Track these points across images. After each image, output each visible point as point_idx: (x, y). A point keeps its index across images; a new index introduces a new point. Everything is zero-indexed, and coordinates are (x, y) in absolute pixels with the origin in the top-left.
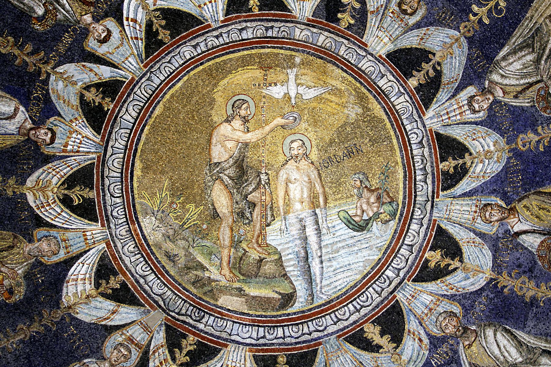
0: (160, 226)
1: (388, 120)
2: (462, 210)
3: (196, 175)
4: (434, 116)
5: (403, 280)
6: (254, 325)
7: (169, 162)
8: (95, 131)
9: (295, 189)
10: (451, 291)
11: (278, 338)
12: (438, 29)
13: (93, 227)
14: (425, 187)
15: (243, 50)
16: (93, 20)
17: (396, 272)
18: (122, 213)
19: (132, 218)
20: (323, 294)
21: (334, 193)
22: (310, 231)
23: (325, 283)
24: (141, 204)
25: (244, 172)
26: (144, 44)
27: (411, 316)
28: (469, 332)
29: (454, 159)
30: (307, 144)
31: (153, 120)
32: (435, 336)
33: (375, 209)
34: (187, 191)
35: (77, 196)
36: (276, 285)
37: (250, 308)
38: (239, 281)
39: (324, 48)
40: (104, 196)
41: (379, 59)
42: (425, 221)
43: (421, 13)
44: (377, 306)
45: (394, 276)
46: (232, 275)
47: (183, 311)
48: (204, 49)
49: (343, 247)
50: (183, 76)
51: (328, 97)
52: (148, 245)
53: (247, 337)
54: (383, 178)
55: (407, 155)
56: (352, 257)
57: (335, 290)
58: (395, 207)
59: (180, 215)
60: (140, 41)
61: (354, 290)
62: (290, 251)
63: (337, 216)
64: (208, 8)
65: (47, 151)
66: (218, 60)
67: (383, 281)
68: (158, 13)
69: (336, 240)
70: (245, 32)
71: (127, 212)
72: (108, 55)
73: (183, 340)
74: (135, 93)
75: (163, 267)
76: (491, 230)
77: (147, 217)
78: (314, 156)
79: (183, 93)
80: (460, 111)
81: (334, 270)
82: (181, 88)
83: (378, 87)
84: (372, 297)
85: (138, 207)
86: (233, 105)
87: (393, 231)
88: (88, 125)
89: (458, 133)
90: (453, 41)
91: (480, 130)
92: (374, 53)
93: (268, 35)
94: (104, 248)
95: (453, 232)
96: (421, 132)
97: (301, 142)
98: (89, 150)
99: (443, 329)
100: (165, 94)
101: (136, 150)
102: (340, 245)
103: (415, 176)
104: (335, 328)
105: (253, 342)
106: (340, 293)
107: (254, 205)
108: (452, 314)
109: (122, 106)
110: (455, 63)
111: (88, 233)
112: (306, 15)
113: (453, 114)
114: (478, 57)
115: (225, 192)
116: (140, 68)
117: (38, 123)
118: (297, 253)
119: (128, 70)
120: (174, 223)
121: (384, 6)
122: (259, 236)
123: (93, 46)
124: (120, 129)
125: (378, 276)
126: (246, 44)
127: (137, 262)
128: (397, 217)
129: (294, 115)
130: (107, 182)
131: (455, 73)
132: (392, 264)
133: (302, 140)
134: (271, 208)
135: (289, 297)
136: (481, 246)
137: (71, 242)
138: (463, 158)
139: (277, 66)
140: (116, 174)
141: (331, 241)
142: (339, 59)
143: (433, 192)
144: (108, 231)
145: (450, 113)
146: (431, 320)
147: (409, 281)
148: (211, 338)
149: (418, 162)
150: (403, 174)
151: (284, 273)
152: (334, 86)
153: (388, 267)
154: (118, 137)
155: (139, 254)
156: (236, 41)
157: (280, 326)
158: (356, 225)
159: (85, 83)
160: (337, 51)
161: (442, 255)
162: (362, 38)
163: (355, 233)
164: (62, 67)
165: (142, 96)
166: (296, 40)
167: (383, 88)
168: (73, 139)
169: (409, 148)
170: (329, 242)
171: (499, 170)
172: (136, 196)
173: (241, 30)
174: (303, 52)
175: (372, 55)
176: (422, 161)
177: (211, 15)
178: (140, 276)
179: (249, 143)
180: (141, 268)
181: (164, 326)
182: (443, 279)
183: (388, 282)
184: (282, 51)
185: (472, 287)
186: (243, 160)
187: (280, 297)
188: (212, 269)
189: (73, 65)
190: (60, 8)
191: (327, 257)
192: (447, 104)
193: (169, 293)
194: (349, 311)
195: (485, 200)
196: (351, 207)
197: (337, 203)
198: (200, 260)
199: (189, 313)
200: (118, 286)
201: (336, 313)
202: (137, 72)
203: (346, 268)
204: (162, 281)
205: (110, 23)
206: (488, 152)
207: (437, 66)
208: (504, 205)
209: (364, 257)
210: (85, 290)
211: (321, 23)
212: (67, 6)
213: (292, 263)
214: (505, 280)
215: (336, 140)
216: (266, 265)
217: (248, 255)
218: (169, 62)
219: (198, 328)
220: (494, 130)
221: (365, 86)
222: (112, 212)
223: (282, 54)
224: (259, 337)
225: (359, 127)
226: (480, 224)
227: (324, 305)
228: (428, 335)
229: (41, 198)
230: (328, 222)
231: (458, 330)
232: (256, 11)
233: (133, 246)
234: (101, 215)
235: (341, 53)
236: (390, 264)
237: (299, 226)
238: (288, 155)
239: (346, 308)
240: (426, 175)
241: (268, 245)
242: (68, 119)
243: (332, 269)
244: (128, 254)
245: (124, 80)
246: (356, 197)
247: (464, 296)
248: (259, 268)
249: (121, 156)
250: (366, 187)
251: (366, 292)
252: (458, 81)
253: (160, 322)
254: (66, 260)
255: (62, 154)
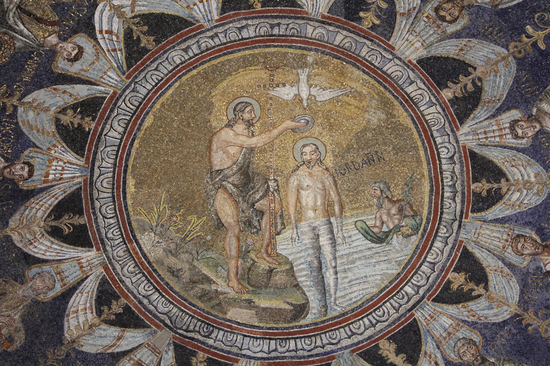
0: (160, 241)
1: (415, 130)
2: (492, 235)
3: (196, 184)
4: (469, 132)
5: (423, 297)
6: (266, 338)
7: (166, 173)
8: (78, 154)
9: (308, 197)
10: (472, 318)
11: (290, 351)
12: (481, 43)
13: (89, 253)
14: (453, 205)
15: (244, 50)
16: (60, 39)
17: (416, 289)
18: (118, 234)
19: (129, 236)
20: (337, 305)
21: (350, 201)
22: (324, 241)
23: (339, 294)
24: (137, 220)
25: (250, 179)
26: (124, 54)
27: (429, 338)
28: (487, 363)
29: (488, 182)
30: (322, 149)
31: (143, 132)
32: (452, 362)
33: (396, 222)
34: (186, 202)
35: (67, 226)
36: (288, 296)
37: (261, 320)
38: (248, 292)
39: (342, 48)
40: (96, 219)
41: (408, 64)
42: (451, 241)
43: (462, 23)
44: (394, 323)
45: (413, 292)
46: (240, 287)
47: (191, 328)
48: (197, 51)
49: (360, 258)
50: (173, 83)
51: (346, 99)
52: (149, 262)
53: (259, 350)
54: (407, 189)
55: (435, 169)
56: (369, 269)
57: (349, 302)
58: (418, 221)
59: (181, 228)
60: (119, 52)
61: (370, 303)
62: (303, 261)
63: (354, 226)
64: (199, 8)
65: (24, 186)
66: (214, 62)
67: (401, 297)
68: (137, 20)
69: (352, 250)
70: (245, 30)
71: (123, 231)
72: (83, 73)
73: (193, 358)
74: (119, 107)
75: (167, 284)
76: (523, 263)
77: (146, 234)
78: (329, 161)
79: (176, 101)
80: (500, 134)
81: (350, 282)
82: (172, 96)
83: (406, 93)
84: (389, 312)
85: (134, 224)
86: (235, 110)
87: (414, 246)
88: (68, 150)
89: (496, 156)
90: (499, 58)
91: (522, 158)
92: (402, 57)
93: (274, 33)
94: (102, 272)
95: (480, 256)
96: (452, 147)
97: (314, 147)
98: (73, 175)
99: (461, 355)
100: (154, 103)
101: (126, 166)
102: (356, 256)
103: (443, 193)
104: (349, 342)
105: (265, 355)
106: (355, 306)
107: (261, 213)
108: (471, 342)
109: (105, 124)
110: (500, 82)
111: (83, 261)
112: (320, 11)
113: (492, 134)
114: (527, 81)
115: (229, 201)
116: (122, 81)
117: (11, 161)
118: (310, 264)
119: (108, 85)
120: (176, 237)
121: (417, 10)
122: (268, 246)
123: (64, 67)
124: (106, 147)
125: (396, 291)
126: (246, 44)
127: (139, 282)
128: (420, 232)
129: (306, 118)
130: (97, 204)
131: (498, 93)
132: (412, 280)
133: (315, 145)
134: (281, 216)
135: (301, 308)
136: (509, 277)
137: (66, 274)
138: (498, 183)
139: (285, 65)
140: (106, 195)
141: (347, 252)
142: (360, 60)
143: (462, 212)
144: (104, 255)
145: (489, 132)
146: (449, 344)
147: (428, 300)
148: (221, 353)
149: (447, 178)
150: (429, 188)
151: (295, 283)
152: (353, 88)
153: (407, 283)
154: (104, 156)
155: (140, 273)
156: (235, 41)
157: (292, 338)
158: (375, 236)
159: (60, 107)
160: (357, 52)
161: (466, 279)
162: (389, 40)
163: (373, 245)
164: (29, 96)
165: (128, 109)
166: (309, 38)
167: (412, 95)
168: (54, 168)
169: (438, 162)
170: (344, 253)
171: (538, 203)
172: (131, 214)
173: (240, 29)
174: (316, 51)
175: (400, 59)
176: (452, 178)
177: (203, 16)
178: (144, 296)
179: (255, 147)
180: (144, 288)
181: (172, 345)
182: (466, 304)
183: (406, 298)
184: (292, 50)
185: (495, 318)
186: (248, 167)
187: (292, 308)
188: (220, 281)
189: (42, 91)
190: (17, 35)
191: (342, 268)
192: (486, 123)
193: (175, 310)
194: (365, 325)
195: (518, 231)
196: (369, 217)
197: (355, 212)
198: (205, 273)
199: (197, 329)
200: (121, 310)
201: (351, 326)
202: (119, 85)
203: (362, 281)
204: (166, 299)
205: (81, 40)
206: (528, 182)
207: (477, 81)
208: (539, 240)
209: (382, 270)
210: (87, 320)
211: (338, 21)
212: (26, 31)
213: (304, 273)
214: (529, 318)
215: (355, 146)
216: (276, 276)
217: (256, 265)
218: (156, 69)
219: (207, 344)
220: (537, 161)
221: (390, 91)
222: (106, 234)
223: (291, 54)
224: (271, 350)
225: (381, 133)
226: (510, 254)
227: (338, 317)
228: (444, 359)
229: (28, 236)
230: (344, 231)
231: (476, 359)
232: (259, 7)
233: (133, 266)
234: (95, 239)
235: (363, 54)
236: (409, 280)
237: (311, 235)
238: (300, 160)
239: (361, 322)
240: (455, 193)
241: (278, 255)
242: (45, 148)
243: (347, 280)
244: (128, 275)
245: (104, 95)
246: (375, 207)
247: (486, 326)
248: (269, 279)
249: (110, 175)
250: (387, 197)
251: (383, 307)
252: (501, 101)
253: (168, 342)
254: (64, 292)
255: (43, 185)
